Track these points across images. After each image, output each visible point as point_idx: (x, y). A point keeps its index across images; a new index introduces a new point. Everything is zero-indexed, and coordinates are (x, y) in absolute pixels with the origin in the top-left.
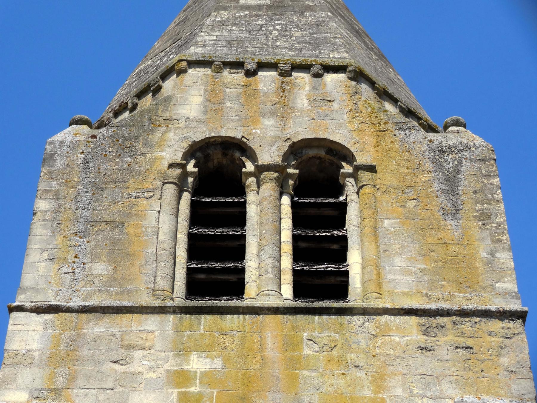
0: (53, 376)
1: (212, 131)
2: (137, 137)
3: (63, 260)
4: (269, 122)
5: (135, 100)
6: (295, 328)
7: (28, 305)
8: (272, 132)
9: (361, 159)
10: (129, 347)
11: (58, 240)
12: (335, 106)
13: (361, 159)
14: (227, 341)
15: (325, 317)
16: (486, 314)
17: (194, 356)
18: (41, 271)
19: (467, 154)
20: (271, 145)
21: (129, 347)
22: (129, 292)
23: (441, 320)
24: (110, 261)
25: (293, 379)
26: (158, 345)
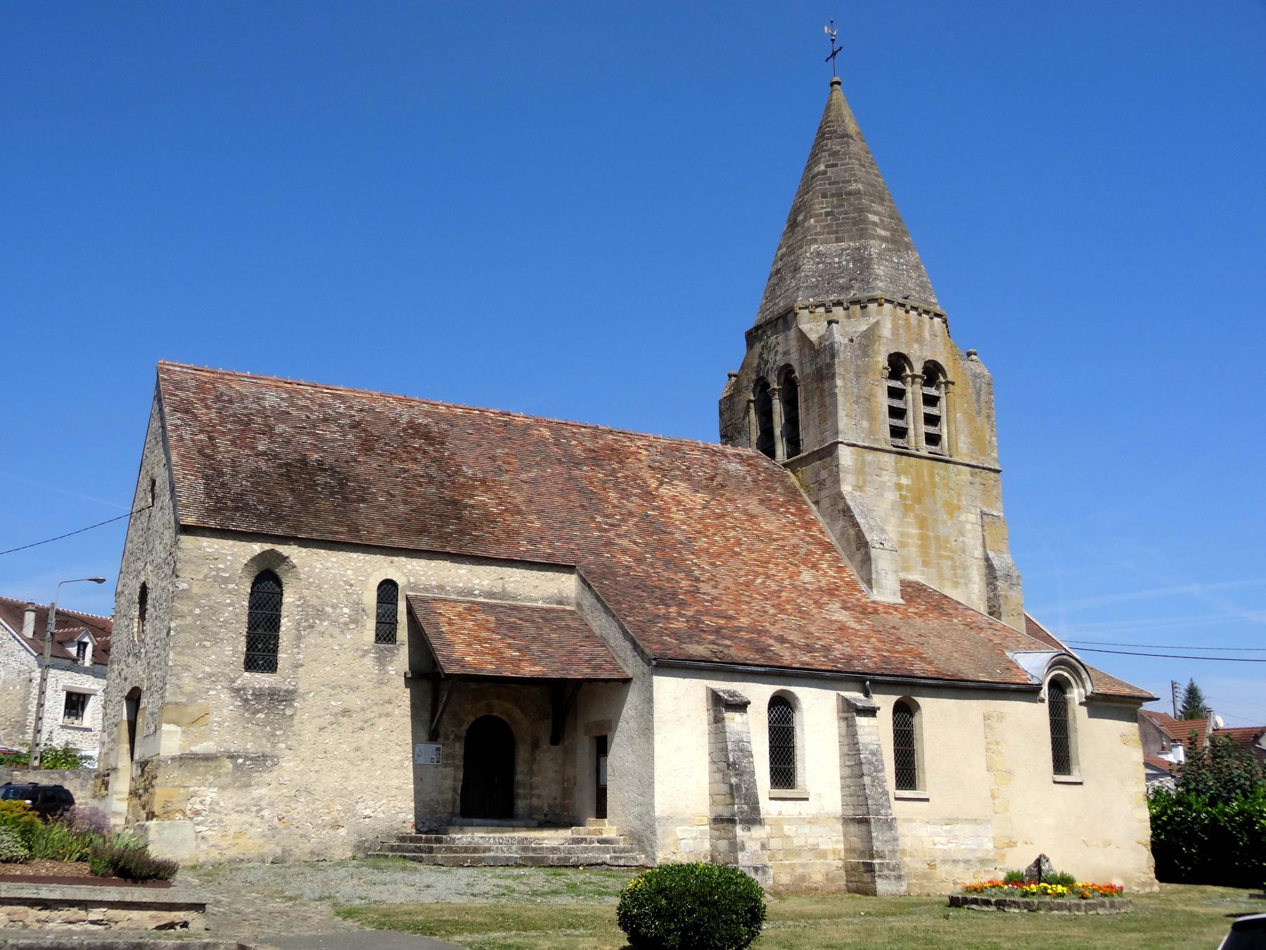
0: (858, 480)
1: (896, 348)
2: (869, 346)
3: (851, 417)
4: (916, 346)
5: (849, 305)
6: (932, 467)
7: (845, 441)
8: (918, 353)
9: (950, 378)
10: (881, 469)
11: (848, 405)
12: (938, 339)
13: (950, 378)
14: (911, 470)
15: (941, 463)
16: (990, 470)
17: (902, 476)
18: (845, 422)
19: (984, 380)
20: (918, 360)
21: (881, 469)
22: (878, 440)
23: (977, 470)
24: (868, 421)
25: (934, 492)
26: (890, 470)
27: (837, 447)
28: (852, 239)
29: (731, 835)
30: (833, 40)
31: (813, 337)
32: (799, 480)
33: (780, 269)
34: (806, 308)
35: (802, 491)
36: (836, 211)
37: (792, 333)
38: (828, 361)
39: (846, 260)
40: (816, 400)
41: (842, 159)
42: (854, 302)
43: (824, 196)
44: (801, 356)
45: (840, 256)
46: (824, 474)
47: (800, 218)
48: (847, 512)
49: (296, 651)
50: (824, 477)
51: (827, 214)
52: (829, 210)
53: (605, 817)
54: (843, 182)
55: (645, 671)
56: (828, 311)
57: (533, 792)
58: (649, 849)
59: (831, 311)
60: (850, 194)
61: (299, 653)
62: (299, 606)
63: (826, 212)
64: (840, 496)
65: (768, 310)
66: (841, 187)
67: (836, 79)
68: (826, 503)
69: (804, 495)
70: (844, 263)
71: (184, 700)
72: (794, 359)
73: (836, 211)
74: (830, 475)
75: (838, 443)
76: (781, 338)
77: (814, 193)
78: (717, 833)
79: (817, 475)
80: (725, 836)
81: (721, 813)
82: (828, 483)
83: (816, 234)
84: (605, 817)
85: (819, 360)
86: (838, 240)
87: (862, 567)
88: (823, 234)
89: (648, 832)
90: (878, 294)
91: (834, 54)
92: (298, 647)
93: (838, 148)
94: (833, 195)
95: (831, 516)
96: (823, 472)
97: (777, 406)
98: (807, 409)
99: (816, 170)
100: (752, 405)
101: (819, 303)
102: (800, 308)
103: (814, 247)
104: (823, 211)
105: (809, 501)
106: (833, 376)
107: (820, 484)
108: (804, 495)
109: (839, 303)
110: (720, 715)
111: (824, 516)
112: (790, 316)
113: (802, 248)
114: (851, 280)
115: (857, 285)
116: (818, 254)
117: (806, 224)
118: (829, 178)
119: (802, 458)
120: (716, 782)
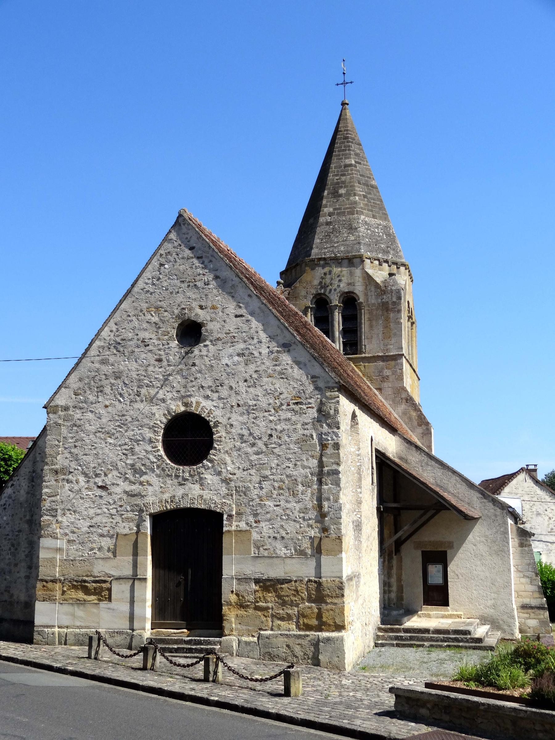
27: (402, 358)
28: (381, 218)
29: (542, 617)
30: (344, 73)
31: (379, 280)
32: (361, 371)
33: (330, 222)
34: (370, 259)
35: (365, 379)
36: (369, 196)
37: (358, 272)
38: (394, 299)
39: (382, 233)
40: (381, 322)
41: (362, 161)
42: (395, 263)
43: (359, 183)
44: (366, 289)
45: (377, 228)
46: (387, 372)
47: (342, 191)
48: (409, 400)
49: (359, 490)
50: (388, 374)
51: (365, 196)
52: (364, 194)
53: (448, 605)
54: (368, 177)
55: (498, 513)
56: (380, 264)
57: (391, 589)
58: (506, 627)
59: (382, 265)
60: (372, 186)
61: (361, 493)
62: (359, 455)
63: (363, 195)
64: (404, 389)
65: (326, 248)
66: (367, 181)
67: (347, 102)
68: (389, 391)
69: (367, 382)
70: (381, 234)
71: (345, 532)
72: (359, 289)
73: (369, 196)
74: (393, 374)
75: (403, 355)
76: (345, 271)
77: (351, 178)
78: (527, 615)
79: (380, 372)
80: (536, 617)
81: (528, 603)
82: (391, 379)
83: (361, 208)
84: (448, 605)
85: (385, 297)
86: (374, 217)
87: (423, 437)
88: (365, 209)
89: (505, 617)
90: (403, 260)
91: (344, 83)
92: (360, 487)
93: (358, 151)
94: (364, 184)
95: (393, 401)
96: (386, 370)
97: (338, 318)
98: (371, 326)
99: (347, 162)
100: (309, 309)
101: (377, 258)
102: (366, 258)
103: (362, 217)
104: (361, 193)
105: (372, 387)
106: (399, 311)
107: (383, 378)
108: (367, 382)
109: (386, 261)
110: (528, 543)
111: (386, 399)
112: (356, 261)
113: (353, 214)
114: (388, 247)
115: (392, 252)
116: (366, 222)
117: (351, 198)
118: (358, 171)
119: (365, 358)
120: (522, 583)
